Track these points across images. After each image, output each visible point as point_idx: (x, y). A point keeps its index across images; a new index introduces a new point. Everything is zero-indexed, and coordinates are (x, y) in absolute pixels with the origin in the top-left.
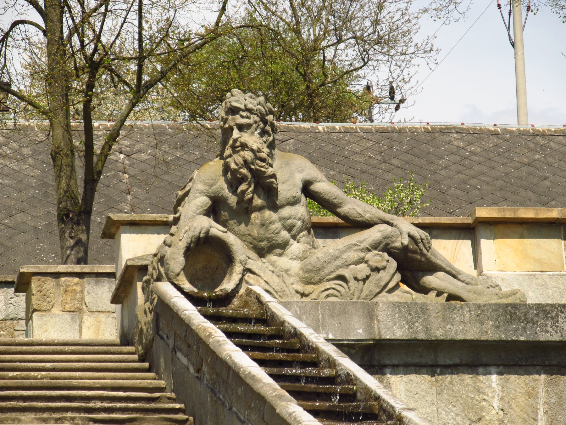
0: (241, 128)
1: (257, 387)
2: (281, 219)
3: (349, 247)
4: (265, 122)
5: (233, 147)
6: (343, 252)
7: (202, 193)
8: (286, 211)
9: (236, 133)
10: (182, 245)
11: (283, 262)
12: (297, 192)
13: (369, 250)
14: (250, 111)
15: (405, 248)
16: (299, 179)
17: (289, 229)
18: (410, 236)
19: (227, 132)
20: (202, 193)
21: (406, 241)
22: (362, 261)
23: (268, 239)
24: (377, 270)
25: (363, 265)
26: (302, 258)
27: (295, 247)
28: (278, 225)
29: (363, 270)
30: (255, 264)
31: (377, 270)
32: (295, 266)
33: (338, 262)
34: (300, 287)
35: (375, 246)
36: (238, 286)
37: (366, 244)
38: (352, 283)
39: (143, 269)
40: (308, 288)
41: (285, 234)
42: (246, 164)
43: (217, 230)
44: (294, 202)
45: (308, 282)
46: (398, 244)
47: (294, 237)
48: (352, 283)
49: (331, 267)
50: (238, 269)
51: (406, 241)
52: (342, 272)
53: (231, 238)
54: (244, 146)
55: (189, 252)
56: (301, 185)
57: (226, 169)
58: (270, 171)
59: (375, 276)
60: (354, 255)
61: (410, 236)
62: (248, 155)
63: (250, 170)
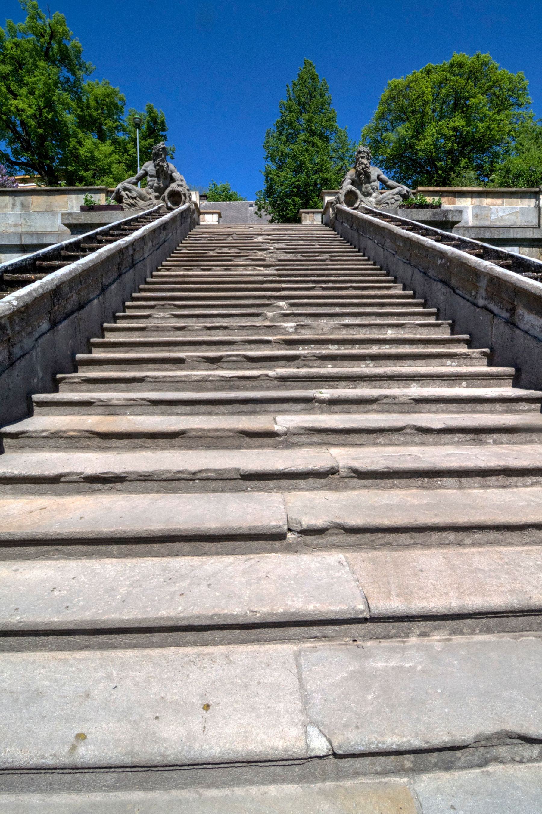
0: (362, 158)
1: (381, 225)
2: (371, 186)
3: (390, 194)
4: (369, 155)
5: (359, 164)
6: (388, 195)
7: (349, 179)
8: (373, 184)
9: (360, 159)
10: (344, 193)
11: (371, 199)
12: (376, 178)
13: (395, 195)
14: (364, 152)
15: (405, 194)
16: (376, 174)
17: (373, 189)
18: (407, 191)
19: (358, 159)
20: (349, 179)
21: (405, 192)
22: (393, 198)
23: (367, 192)
24: (397, 201)
25: (393, 200)
26: (375, 198)
27: (374, 195)
28: (370, 188)
29: (393, 201)
30: (363, 199)
31: (397, 201)
32: (374, 200)
33: (386, 199)
34: (375, 206)
35: (397, 194)
36: (359, 205)
37: (394, 193)
38: (390, 205)
39: (332, 203)
40: (378, 206)
41: (372, 191)
42: (363, 169)
43: (354, 189)
44: (374, 181)
45: (377, 204)
46: (403, 193)
47: (374, 192)
48: (390, 205)
49: (384, 200)
50: (359, 200)
51: (405, 192)
52: (387, 201)
53: (358, 191)
54: (363, 163)
55: (346, 195)
56: (377, 176)
57: (357, 171)
58: (369, 171)
59: (396, 203)
60: (391, 196)
61: (407, 191)
62: (363, 166)
63: (364, 171)
